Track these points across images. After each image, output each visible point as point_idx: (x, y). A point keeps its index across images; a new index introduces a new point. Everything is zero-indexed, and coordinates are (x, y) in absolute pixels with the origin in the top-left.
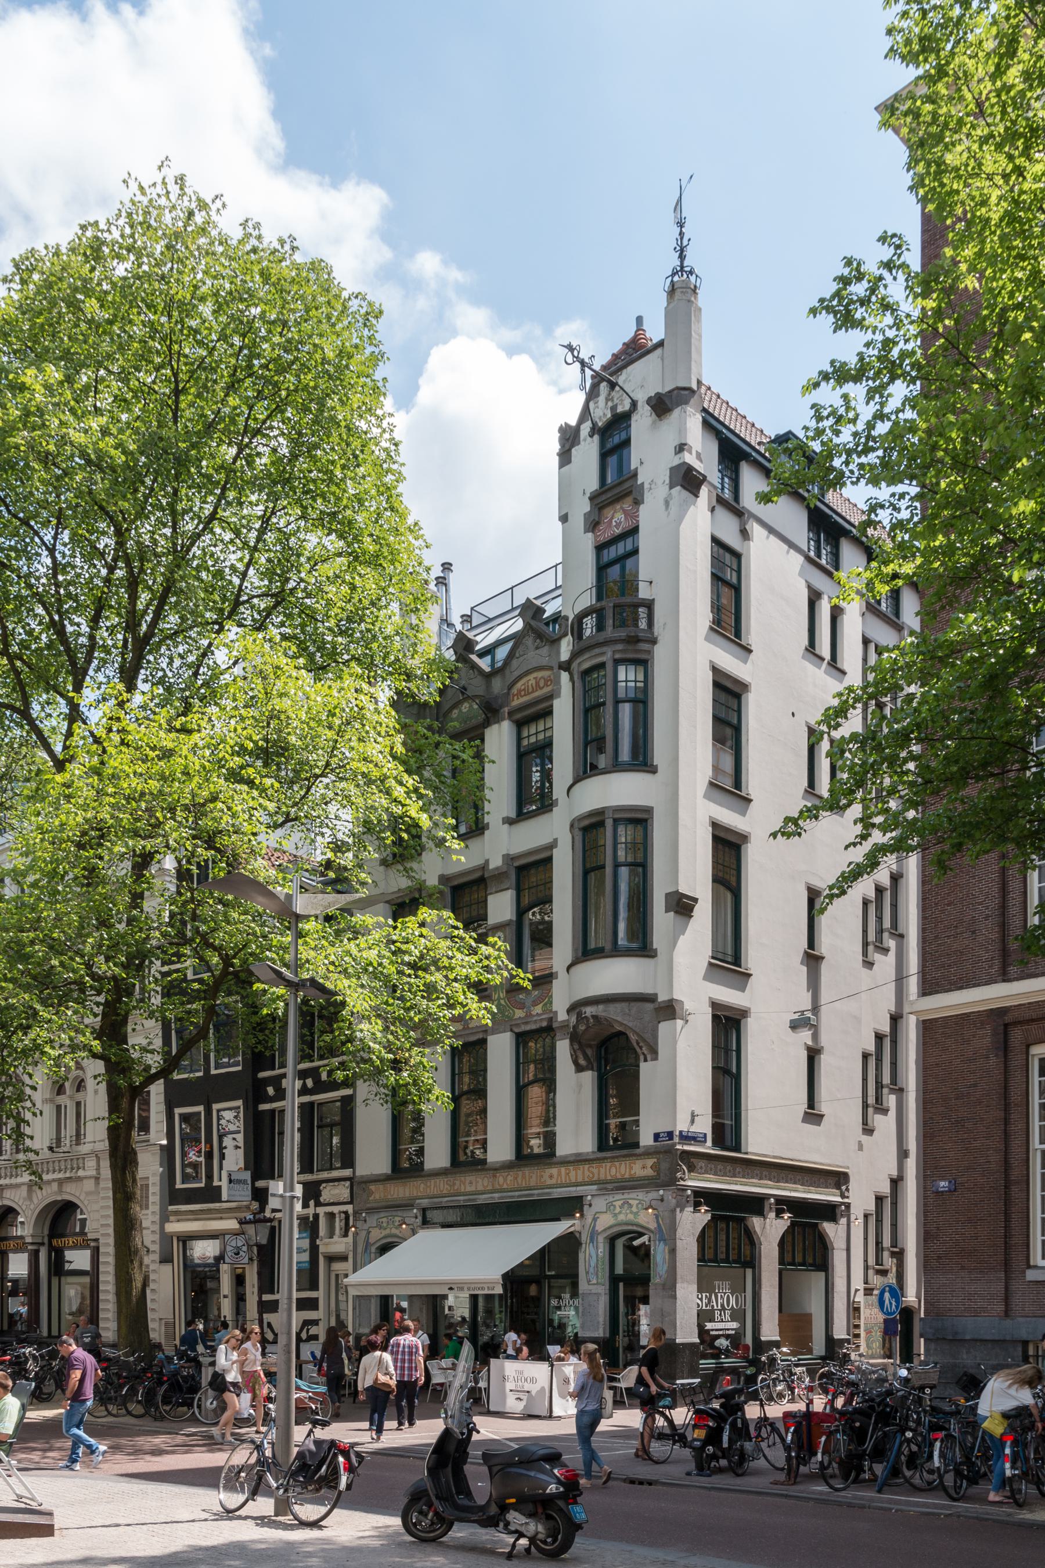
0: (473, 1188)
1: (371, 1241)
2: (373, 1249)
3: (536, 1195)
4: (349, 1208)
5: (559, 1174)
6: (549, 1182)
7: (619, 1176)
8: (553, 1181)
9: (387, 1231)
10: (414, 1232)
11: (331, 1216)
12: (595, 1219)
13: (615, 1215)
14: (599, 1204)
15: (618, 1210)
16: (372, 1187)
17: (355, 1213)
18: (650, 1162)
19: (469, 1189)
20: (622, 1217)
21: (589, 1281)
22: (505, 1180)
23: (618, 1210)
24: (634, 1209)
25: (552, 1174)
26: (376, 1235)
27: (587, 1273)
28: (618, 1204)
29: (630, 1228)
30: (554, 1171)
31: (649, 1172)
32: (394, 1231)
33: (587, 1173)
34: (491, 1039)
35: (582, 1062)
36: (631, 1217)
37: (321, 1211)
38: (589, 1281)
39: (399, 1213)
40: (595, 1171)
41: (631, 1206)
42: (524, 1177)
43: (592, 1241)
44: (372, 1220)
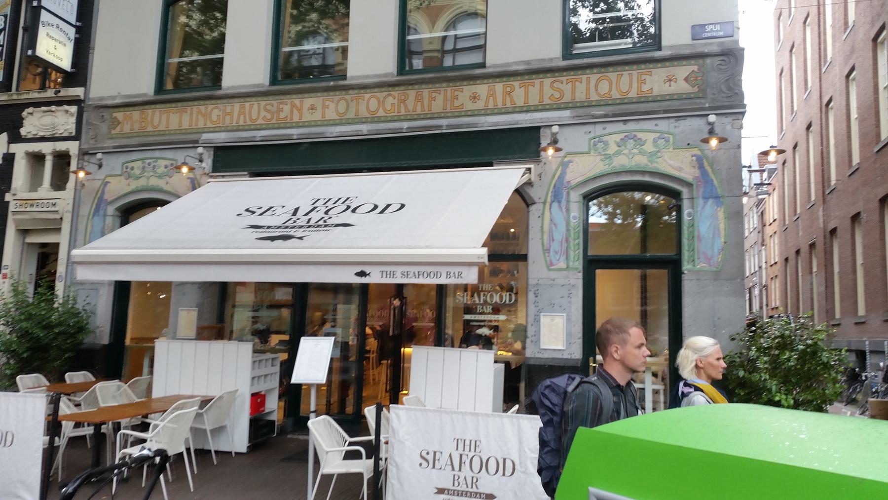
0: (317, 116)
1: (108, 197)
2: (111, 210)
3: (445, 125)
4: (72, 147)
5: (492, 94)
6: (470, 106)
7: (615, 95)
8: (480, 105)
9: (142, 182)
10: (194, 185)
11: (37, 159)
12: (564, 165)
15: (613, 149)
16: (119, 115)
17: (84, 153)
18: (683, 71)
19: (307, 117)
20: (622, 161)
21: (550, 265)
22: (381, 103)
23: (613, 149)
24: (649, 147)
25: (467, 96)
26: (120, 188)
28: (613, 140)
29: (647, 178)
30: (482, 89)
31: (681, 87)
32: (154, 182)
33: (548, 91)
36: (640, 161)
37: (20, 150)
38: (550, 265)
39: (169, 154)
40: (567, 88)
41: (640, 143)
42: (419, 99)
43: (557, 197)
44: (114, 163)
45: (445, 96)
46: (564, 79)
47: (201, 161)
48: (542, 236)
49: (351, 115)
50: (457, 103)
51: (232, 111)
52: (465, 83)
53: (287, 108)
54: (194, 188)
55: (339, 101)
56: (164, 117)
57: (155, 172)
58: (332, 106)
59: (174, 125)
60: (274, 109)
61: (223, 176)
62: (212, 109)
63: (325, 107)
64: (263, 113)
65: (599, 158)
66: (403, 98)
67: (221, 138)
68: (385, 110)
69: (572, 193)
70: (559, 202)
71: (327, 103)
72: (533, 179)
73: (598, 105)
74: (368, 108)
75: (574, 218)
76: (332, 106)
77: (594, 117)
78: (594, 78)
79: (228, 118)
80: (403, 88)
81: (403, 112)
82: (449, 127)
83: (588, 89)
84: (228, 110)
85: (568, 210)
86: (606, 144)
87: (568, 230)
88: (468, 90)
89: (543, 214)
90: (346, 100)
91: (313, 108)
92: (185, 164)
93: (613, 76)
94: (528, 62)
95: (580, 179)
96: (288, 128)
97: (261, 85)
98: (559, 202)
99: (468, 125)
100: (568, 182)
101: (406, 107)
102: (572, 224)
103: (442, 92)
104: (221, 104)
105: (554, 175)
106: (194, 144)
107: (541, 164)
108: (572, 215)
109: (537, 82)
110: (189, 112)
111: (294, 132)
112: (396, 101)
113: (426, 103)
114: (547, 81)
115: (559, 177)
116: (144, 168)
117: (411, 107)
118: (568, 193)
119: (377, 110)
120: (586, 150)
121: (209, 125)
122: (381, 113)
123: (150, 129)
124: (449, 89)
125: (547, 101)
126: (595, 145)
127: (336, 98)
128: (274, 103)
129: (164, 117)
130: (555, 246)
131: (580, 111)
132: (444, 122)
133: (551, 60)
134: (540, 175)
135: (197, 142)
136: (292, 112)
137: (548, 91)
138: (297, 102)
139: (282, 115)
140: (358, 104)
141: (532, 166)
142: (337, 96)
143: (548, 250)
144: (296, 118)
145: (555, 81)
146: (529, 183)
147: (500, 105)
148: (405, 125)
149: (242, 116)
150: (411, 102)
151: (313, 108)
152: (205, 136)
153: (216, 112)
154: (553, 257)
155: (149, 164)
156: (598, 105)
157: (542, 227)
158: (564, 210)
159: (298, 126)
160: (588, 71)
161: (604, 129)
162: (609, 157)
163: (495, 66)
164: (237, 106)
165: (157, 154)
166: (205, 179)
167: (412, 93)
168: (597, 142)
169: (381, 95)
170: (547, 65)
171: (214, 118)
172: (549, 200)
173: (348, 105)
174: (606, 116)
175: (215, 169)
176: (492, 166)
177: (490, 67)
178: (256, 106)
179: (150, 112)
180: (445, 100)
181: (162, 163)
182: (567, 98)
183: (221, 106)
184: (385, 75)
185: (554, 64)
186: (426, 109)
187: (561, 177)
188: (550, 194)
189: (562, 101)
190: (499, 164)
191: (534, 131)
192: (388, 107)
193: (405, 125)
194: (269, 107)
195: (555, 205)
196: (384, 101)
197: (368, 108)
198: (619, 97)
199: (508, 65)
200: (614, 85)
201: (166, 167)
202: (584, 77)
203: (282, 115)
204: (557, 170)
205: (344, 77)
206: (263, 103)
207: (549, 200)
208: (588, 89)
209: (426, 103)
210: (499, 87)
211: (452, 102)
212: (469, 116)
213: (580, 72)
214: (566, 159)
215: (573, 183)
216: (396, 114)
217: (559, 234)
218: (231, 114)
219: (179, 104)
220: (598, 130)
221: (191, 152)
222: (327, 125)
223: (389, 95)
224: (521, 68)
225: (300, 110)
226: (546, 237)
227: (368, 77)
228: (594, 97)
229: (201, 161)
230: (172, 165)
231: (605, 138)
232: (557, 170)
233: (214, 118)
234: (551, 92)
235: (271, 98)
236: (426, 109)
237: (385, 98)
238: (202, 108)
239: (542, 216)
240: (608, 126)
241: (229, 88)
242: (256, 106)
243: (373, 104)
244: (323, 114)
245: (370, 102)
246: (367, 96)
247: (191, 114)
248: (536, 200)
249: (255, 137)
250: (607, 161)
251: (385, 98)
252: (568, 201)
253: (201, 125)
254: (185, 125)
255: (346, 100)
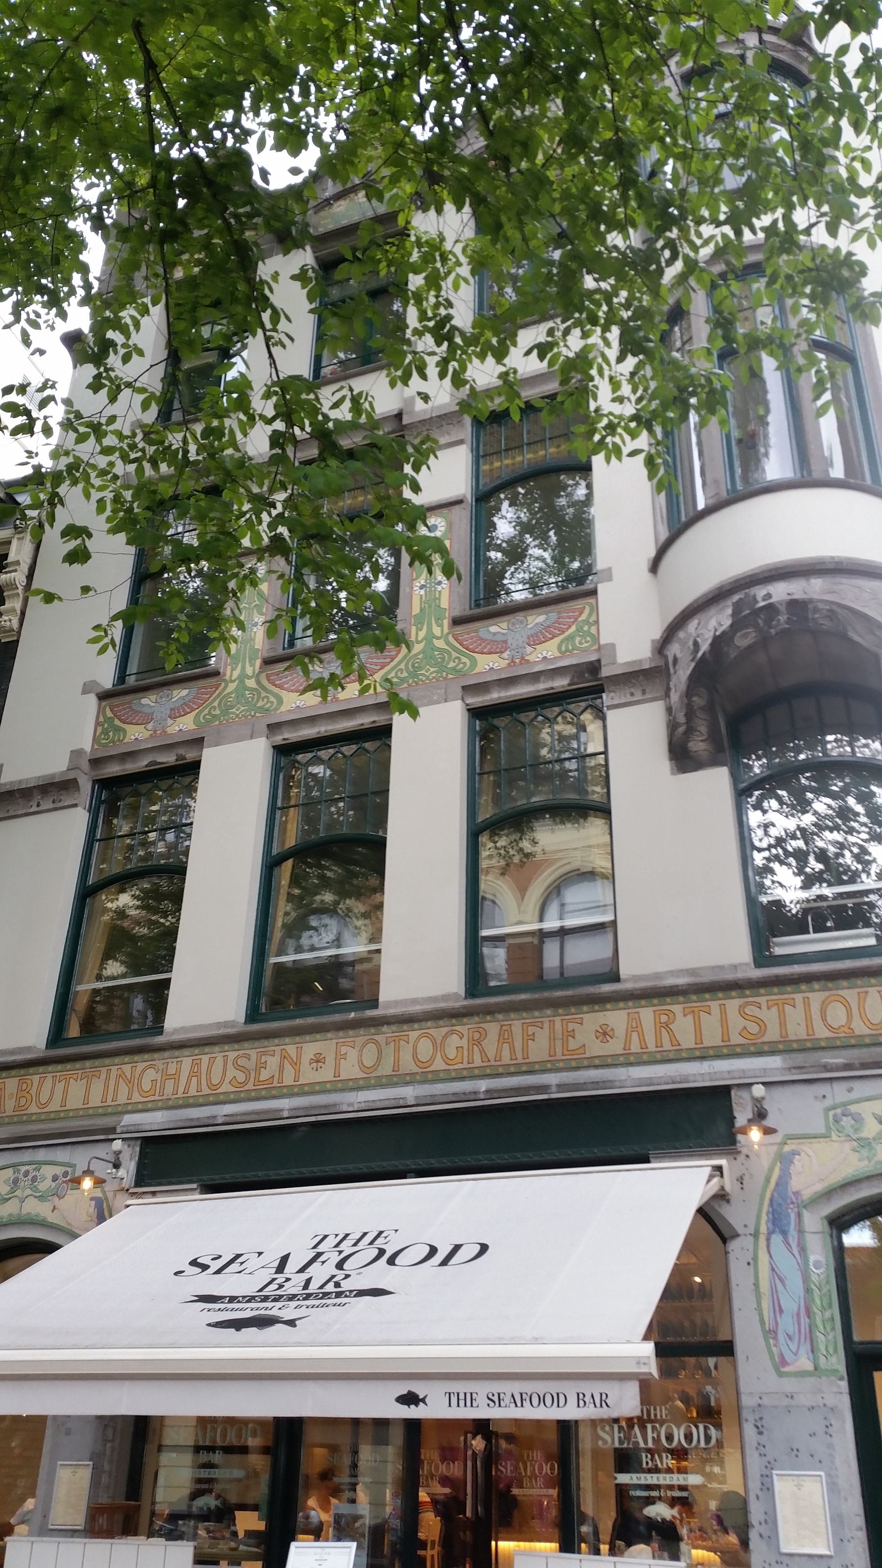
0: (326, 1074)
3: (555, 1083)
5: (635, 1027)
6: (597, 1049)
8: (615, 1047)
12: (785, 1160)
13: (864, 1144)
14: (795, 1109)
19: (309, 1076)
22: (439, 1046)
25: (588, 1030)
27: (771, 1333)
30: (616, 1018)
32: (33, 1207)
33: (736, 1022)
34: (400, 722)
35: (698, 746)
39: (61, 1155)
40: (770, 1016)
42: (505, 1037)
43: (778, 1223)
45: (552, 1030)
46: (762, 1000)
47: (117, 1166)
48: (759, 1303)
49: (386, 1069)
50: (573, 1044)
51: (178, 1072)
52: (585, 1008)
53: (273, 1062)
54: (101, 1218)
55: (364, 1046)
56: (60, 1086)
57: (35, 1189)
58: (353, 1054)
59: (75, 1101)
60: (251, 1065)
61: (154, 1193)
62: (144, 1070)
63: (340, 1057)
64: (231, 1072)
65: (847, 1146)
66: (477, 1035)
67: (156, 1121)
68: (446, 1060)
69: (806, 1214)
70: (784, 1233)
71: (343, 1050)
72: (728, 1188)
73: (831, 1047)
74: (415, 1055)
75: (817, 1265)
76: (353, 1054)
77: (826, 1068)
78: (816, 998)
79: (169, 1085)
80: (476, 1019)
81: (478, 1062)
82: (561, 1087)
83: (808, 1019)
84: (172, 1069)
85: (803, 1250)
86: (858, 1119)
87: (808, 1291)
88: (592, 1020)
89: (755, 1258)
90: (376, 1043)
91: (318, 1060)
92: (88, 1172)
93: (850, 994)
94: (692, 972)
95: (819, 1187)
96: (274, 1097)
97: (232, 1024)
98: (784, 1233)
99: (596, 1084)
100: (797, 1194)
101: (482, 1052)
102: (814, 1278)
103: (546, 1025)
104: (159, 1060)
105: (768, 1180)
106: (108, 1134)
107: (741, 1158)
108: (812, 1258)
109: (714, 1005)
110: (103, 1076)
111: (284, 1104)
112: (464, 1043)
113: (518, 1045)
114: (733, 1004)
115: (777, 1184)
116: (16, 1181)
117: (491, 1052)
118: (799, 1215)
119: (432, 1059)
120: (822, 1130)
121: (137, 1098)
122: (439, 1064)
123: (33, 1109)
124: (558, 1019)
125: (736, 1039)
126: (837, 1121)
127: (360, 1040)
128: (252, 1052)
129: (60, 1086)
130: (787, 1324)
131: (799, 1059)
132: (552, 1079)
133: (735, 967)
134: (741, 1180)
135: (113, 1130)
136: (281, 1068)
137: (736, 1022)
138: (291, 1050)
139: (265, 1075)
140: (397, 1050)
141: (723, 1162)
142: (360, 1037)
143: (771, 1333)
144: (288, 1080)
145: (747, 1004)
146: (721, 1196)
147: (652, 1047)
148: (483, 1085)
149: (194, 1079)
150: (490, 1045)
151: (318, 1060)
152: (128, 1119)
153: (151, 1074)
154: (785, 1347)
155: (26, 1174)
156: (831, 1047)
157: (756, 1285)
158: (795, 1250)
159: (291, 1094)
160: (803, 987)
161: (850, 1090)
162: (864, 1144)
163: (635, 978)
164: (187, 1062)
165: (41, 1155)
166: (123, 1199)
167: (492, 1028)
168: (839, 1118)
169: (438, 1033)
170: (730, 976)
171: (146, 1085)
172: (763, 1229)
173: (380, 1051)
174: (848, 1067)
175: (140, 1181)
176: (648, 1162)
177: (626, 980)
178: (219, 1061)
179: (36, 1078)
180: (552, 1039)
181: (48, 1171)
182: (773, 1034)
183: (160, 1064)
184: (445, 998)
185: (740, 975)
186: (519, 1056)
187: (783, 1182)
188: (764, 1217)
189: (766, 1039)
190: (662, 1157)
191: (719, 1096)
192: (452, 1053)
193: (483, 1085)
194: (242, 1062)
195: (777, 1239)
196: (443, 1044)
197: (415, 1055)
198: (867, 1031)
199: (658, 976)
200: (855, 1012)
201: (55, 1178)
202: (798, 997)
203: (265, 1075)
204: (771, 1170)
205: (374, 1003)
206: (232, 1055)
207: (763, 1229)
208: (808, 1019)
209: (518, 1045)
210: (647, 1014)
211: (565, 1043)
212: (596, 1067)
213: (789, 989)
214: (787, 1148)
215: (807, 1194)
216: (465, 1065)
217: (792, 1298)
218: (176, 1077)
219: (88, 1063)
220: (839, 1093)
221: (101, 1151)
222: (342, 1090)
223: (452, 1032)
224: (682, 981)
225: (296, 1064)
226: (766, 1304)
227: (414, 1001)
228: (822, 1032)
229: (117, 1166)
230: (66, 1174)
231: (853, 1108)
232: (771, 1170)
233: (146, 1085)
234: (742, 1023)
235: (246, 1045)
236: (519, 1056)
237: (445, 1037)
238: (127, 1068)
239: (753, 1263)
240: (857, 1085)
241: (176, 1031)
242: (219, 1061)
243: (425, 1048)
244: (337, 1068)
245: (419, 1047)
246: (413, 1035)
247: (108, 1078)
248: (739, 1229)
249: (215, 1117)
250: (865, 1152)
251: (445, 1037)
252: (801, 1232)
253: (122, 1099)
254: (95, 1101)
255: (376, 1043)
